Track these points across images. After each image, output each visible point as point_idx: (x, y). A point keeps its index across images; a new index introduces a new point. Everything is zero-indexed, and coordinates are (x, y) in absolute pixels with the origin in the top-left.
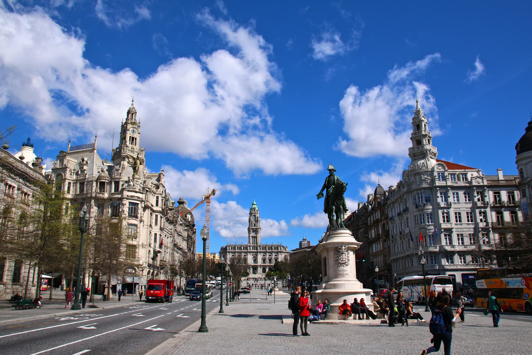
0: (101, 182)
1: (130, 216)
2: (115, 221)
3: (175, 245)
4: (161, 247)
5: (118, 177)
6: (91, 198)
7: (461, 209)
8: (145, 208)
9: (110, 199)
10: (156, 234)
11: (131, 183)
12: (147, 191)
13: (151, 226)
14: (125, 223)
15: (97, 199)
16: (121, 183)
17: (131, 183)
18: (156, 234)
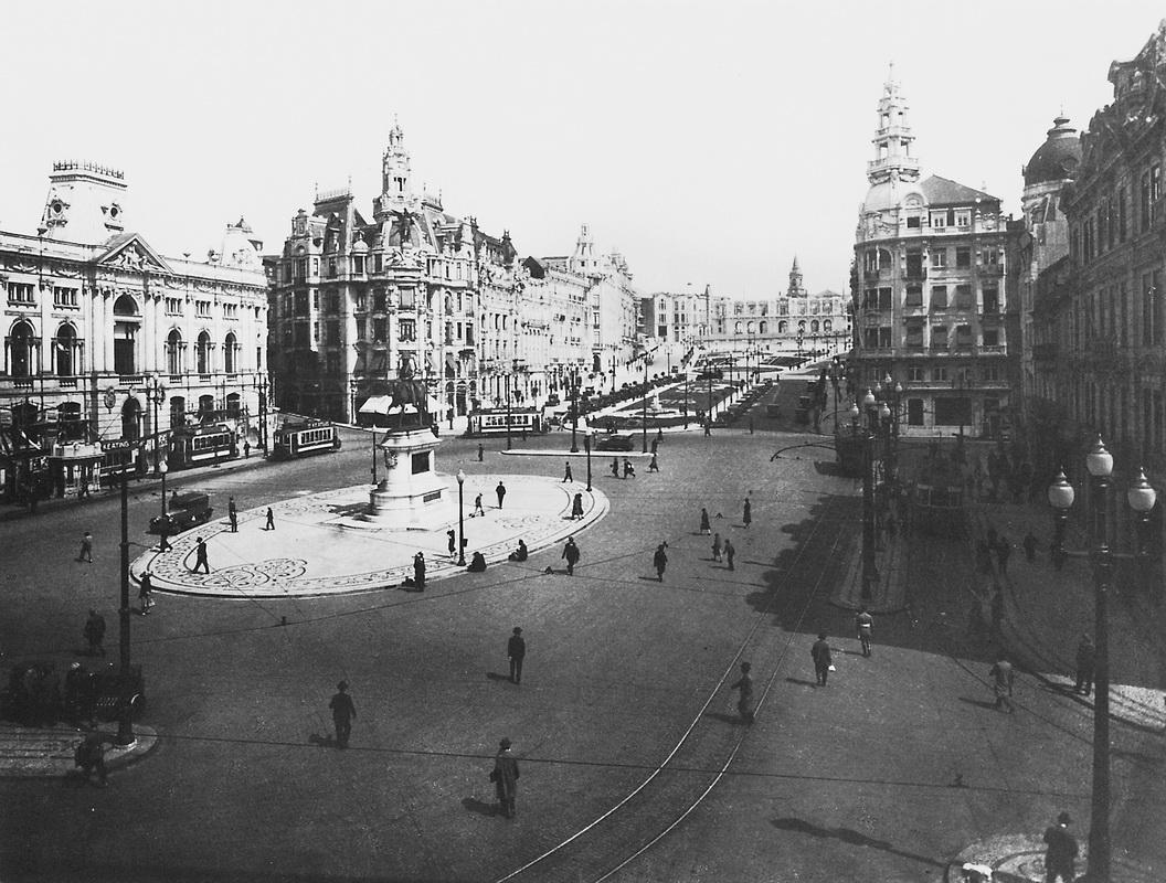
0: (356, 257)
1: (402, 308)
2: (381, 316)
3: (523, 326)
4: (470, 341)
5: (379, 247)
6: (344, 283)
7: (948, 280)
8: (431, 288)
9: (371, 283)
10: (459, 324)
11: (398, 257)
12: (434, 261)
13: (449, 312)
14: (393, 320)
15: (352, 284)
16: (384, 258)
17: (398, 257)
18: (459, 324)
